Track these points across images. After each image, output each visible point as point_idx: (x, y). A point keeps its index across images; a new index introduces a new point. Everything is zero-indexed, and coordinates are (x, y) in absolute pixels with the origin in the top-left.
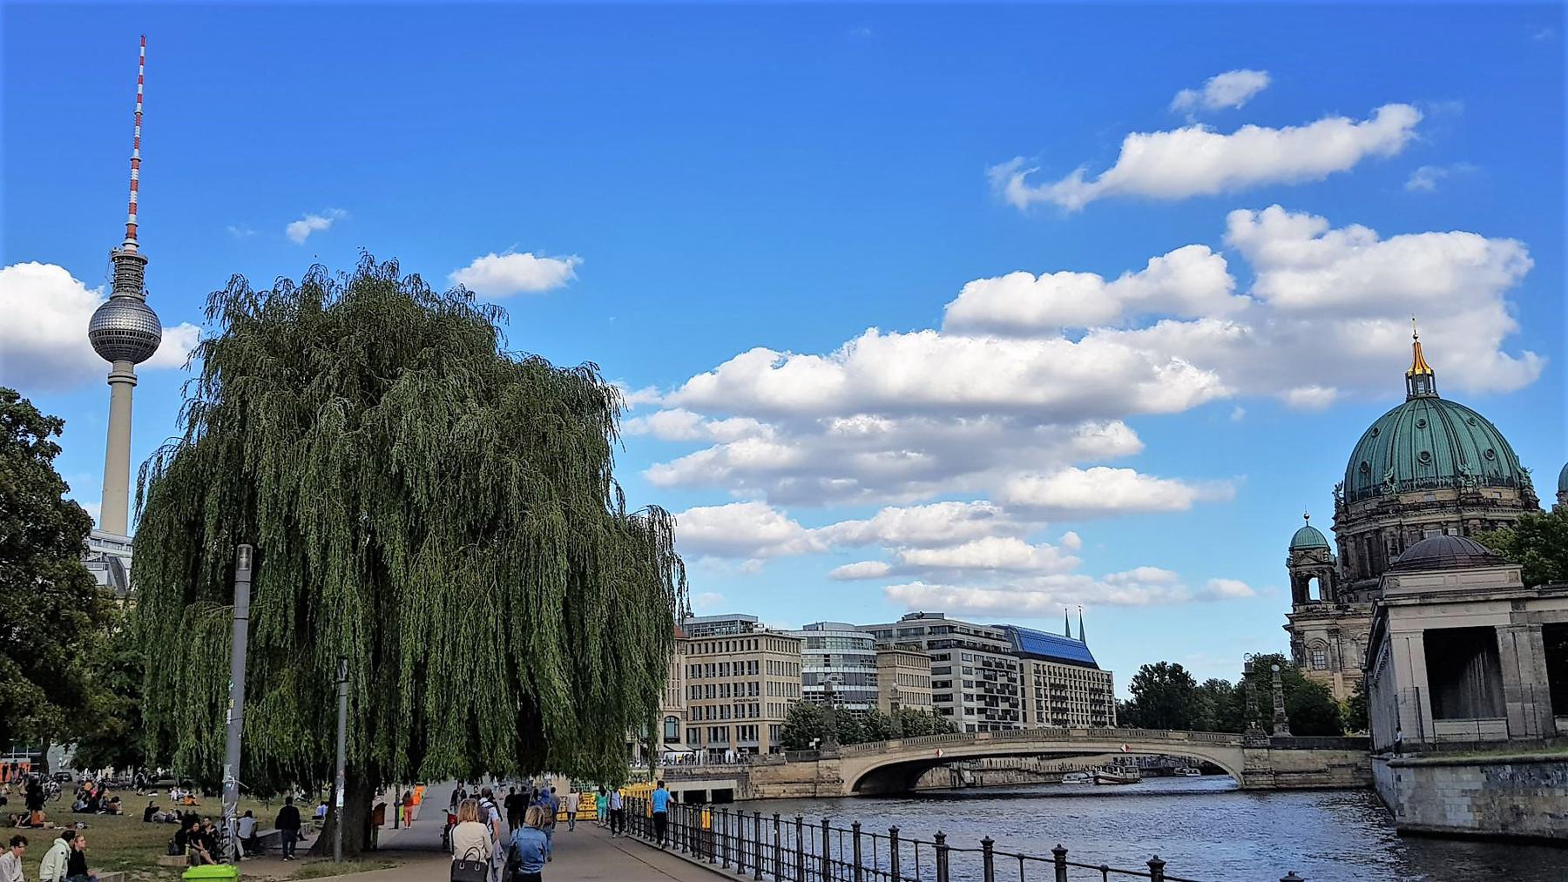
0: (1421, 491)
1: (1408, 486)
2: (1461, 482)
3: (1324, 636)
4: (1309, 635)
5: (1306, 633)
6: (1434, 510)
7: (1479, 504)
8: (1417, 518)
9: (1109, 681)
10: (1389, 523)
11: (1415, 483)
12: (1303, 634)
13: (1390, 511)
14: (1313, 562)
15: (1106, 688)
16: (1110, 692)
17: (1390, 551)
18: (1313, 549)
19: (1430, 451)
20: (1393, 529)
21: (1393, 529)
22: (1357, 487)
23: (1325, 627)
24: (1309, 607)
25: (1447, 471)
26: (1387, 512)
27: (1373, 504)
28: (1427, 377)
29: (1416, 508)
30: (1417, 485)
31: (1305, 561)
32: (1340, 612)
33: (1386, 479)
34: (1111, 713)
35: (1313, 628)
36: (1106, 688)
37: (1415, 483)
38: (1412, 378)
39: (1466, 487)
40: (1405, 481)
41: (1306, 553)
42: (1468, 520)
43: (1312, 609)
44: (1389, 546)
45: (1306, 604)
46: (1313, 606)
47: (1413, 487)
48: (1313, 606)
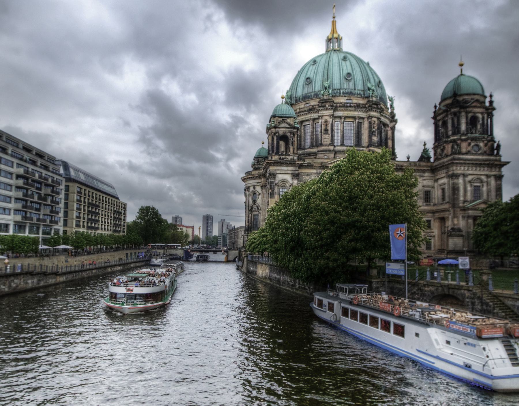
0: (346, 97)
1: (337, 93)
2: (370, 94)
3: (288, 178)
4: (280, 177)
5: (277, 175)
6: (353, 109)
7: (378, 108)
8: (342, 113)
9: (125, 208)
10: (326, 113)
11: (342, 91)
12: (275, 175)
13: (327, 106)
14: (288, 126)
15: (123, 212)
16: (125, 214)
17: (323, 132)
18: (288, 118)
19: (350, 71)
20: (327, 118)
21: (327, 118)
22: (299, 93)
23: (290, 172)
24: (282, 157)
25: (360, 87)
26: (325, 106)
27: (314, 103)
28: (339, 40)
29: (344, 106)
30: (343, 93)
31: (283, 125)
32: (300, 162)
33: (327, 85)
34: (124, 226)
35: (283, 172)
36: (123, 212)
37: (342, 91)
38: (329, 40)
39: (372, 97)
40: (335, 90)
41: (283, 120)
42: (372, 117)
43: (283, 159)
44: (323, 128)
45: (279, 155)
46: (284, 157)
47: (340, 93)
48: (284, 157)
